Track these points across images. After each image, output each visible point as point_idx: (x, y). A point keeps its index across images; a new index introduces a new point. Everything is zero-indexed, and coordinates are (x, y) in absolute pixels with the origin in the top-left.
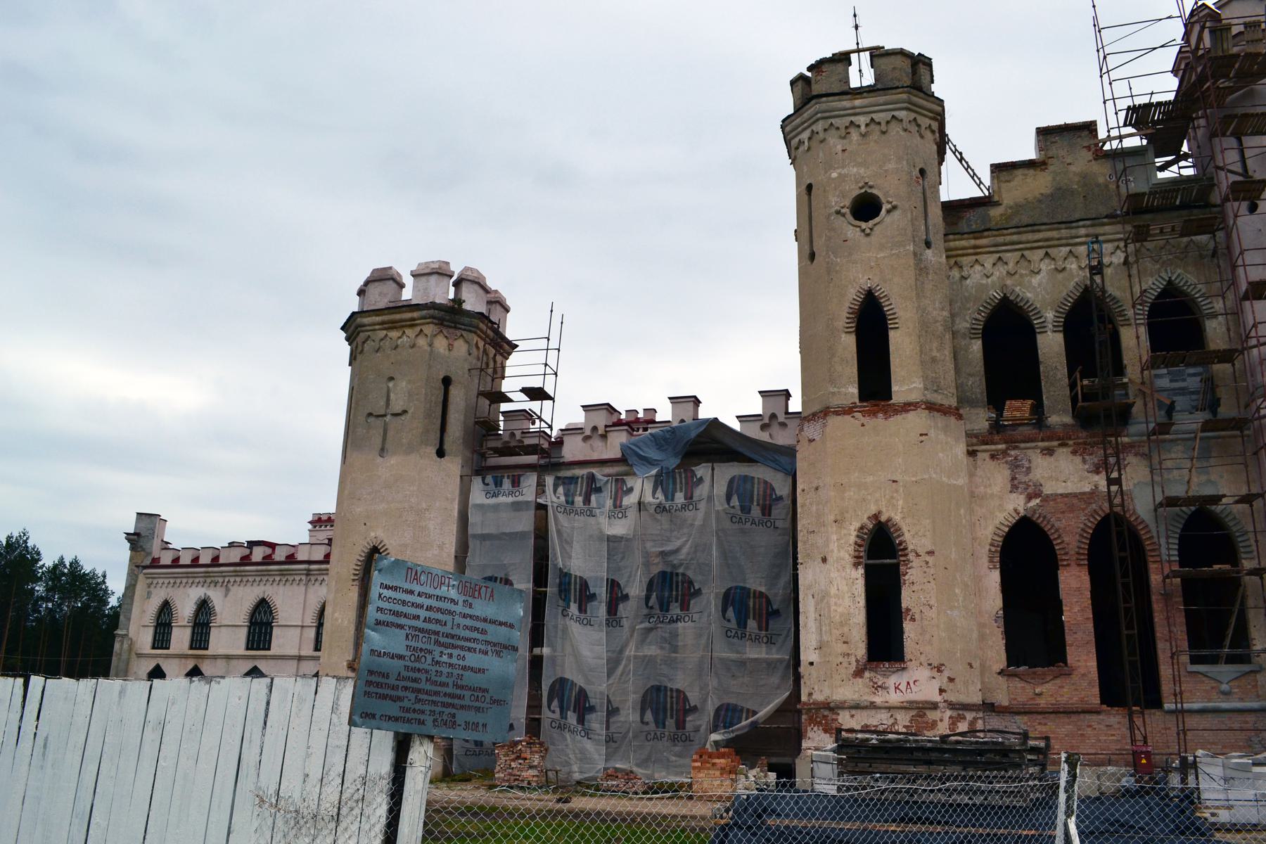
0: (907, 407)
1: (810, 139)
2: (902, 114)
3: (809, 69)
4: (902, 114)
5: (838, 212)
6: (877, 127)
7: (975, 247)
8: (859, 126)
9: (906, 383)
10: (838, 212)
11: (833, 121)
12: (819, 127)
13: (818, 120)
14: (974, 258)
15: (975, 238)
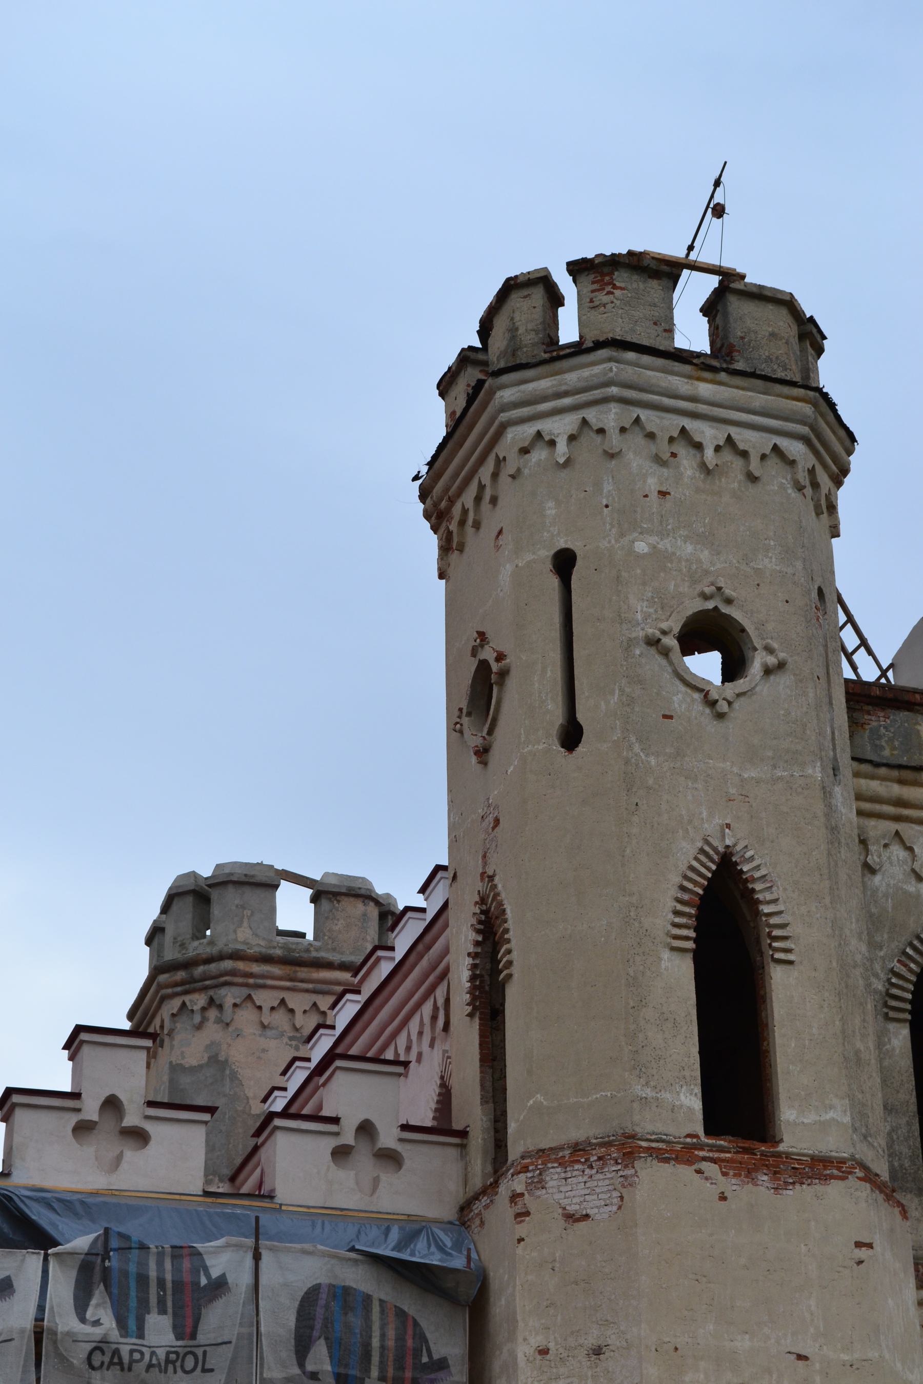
0: (820, 1168)
1: (572, 438)
2: (795, 449)
3: (577, 268)
4: (795, 449)
5: (653, 642)
6: (738, 463)
7: (900, 803)
8: (699, 446)
9: (813, 1106)
10: (653, 642)
11: (644, 414)
12: (610, 417)
13: (605, 400)
14: (893, 826)
15: (901, 782)
